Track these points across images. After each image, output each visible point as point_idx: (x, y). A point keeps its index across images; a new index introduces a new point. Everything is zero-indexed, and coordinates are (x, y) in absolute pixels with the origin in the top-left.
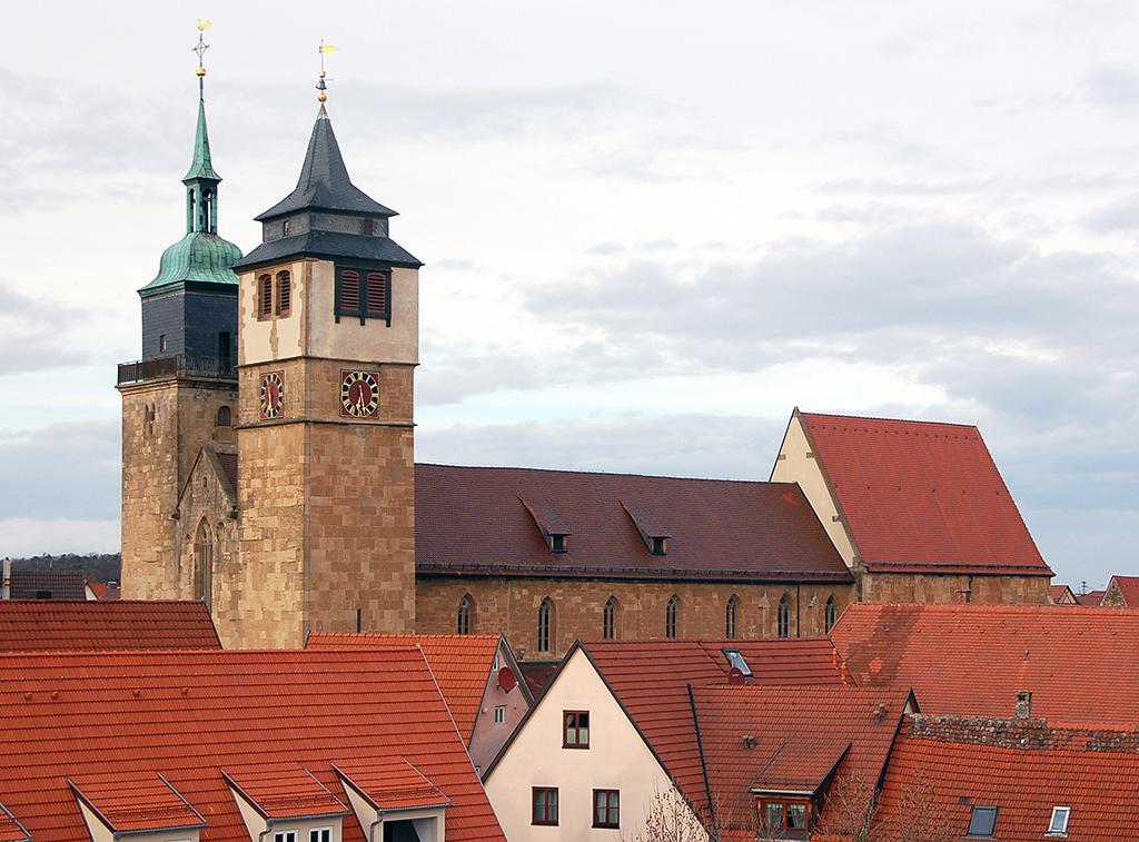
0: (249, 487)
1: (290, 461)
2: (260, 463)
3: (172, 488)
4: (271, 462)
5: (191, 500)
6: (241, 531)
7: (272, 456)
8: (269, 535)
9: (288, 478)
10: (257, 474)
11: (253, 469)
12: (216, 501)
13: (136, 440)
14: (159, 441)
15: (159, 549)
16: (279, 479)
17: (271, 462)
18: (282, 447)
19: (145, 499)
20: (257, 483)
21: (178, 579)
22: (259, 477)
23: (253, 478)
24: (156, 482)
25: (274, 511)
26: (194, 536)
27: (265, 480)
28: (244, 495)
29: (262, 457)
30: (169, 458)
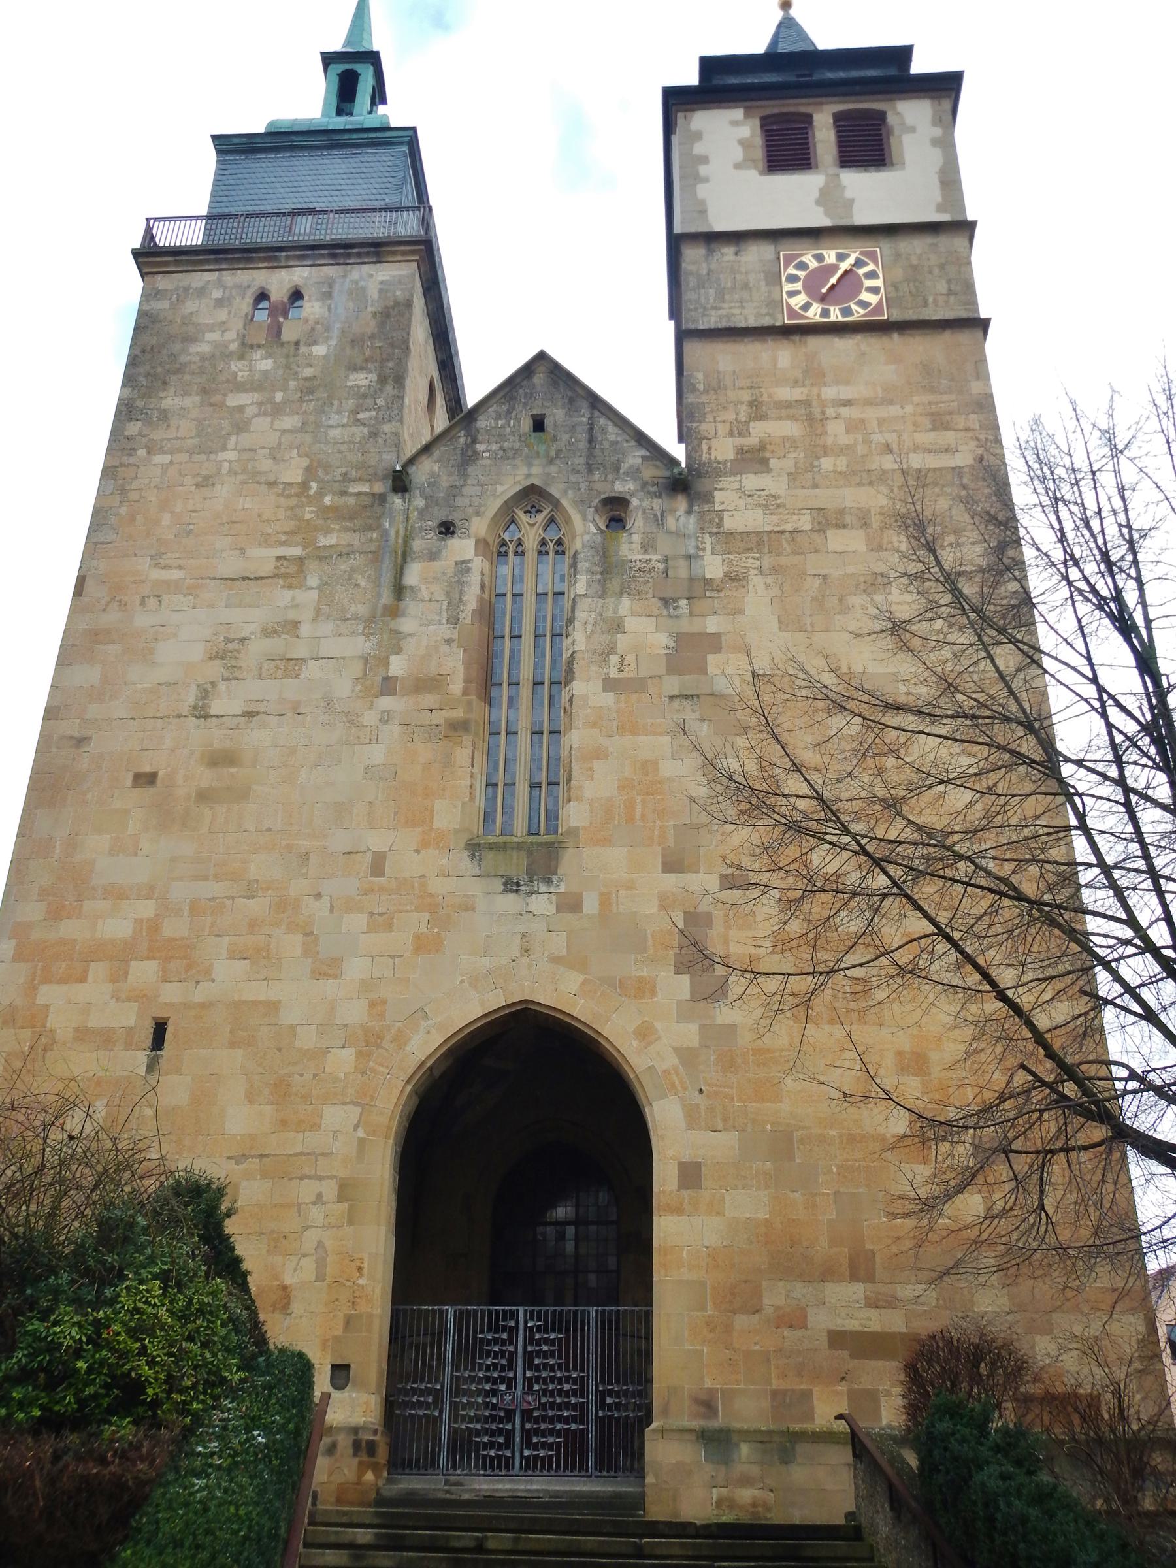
4: (829, 393)
6: (712, 523)
8: (848, 519)
14: (320, 350)
15: (296, 551)
16: (881, 422)
21: (394, 612)
23: (761, 417)
26: (480, 526)
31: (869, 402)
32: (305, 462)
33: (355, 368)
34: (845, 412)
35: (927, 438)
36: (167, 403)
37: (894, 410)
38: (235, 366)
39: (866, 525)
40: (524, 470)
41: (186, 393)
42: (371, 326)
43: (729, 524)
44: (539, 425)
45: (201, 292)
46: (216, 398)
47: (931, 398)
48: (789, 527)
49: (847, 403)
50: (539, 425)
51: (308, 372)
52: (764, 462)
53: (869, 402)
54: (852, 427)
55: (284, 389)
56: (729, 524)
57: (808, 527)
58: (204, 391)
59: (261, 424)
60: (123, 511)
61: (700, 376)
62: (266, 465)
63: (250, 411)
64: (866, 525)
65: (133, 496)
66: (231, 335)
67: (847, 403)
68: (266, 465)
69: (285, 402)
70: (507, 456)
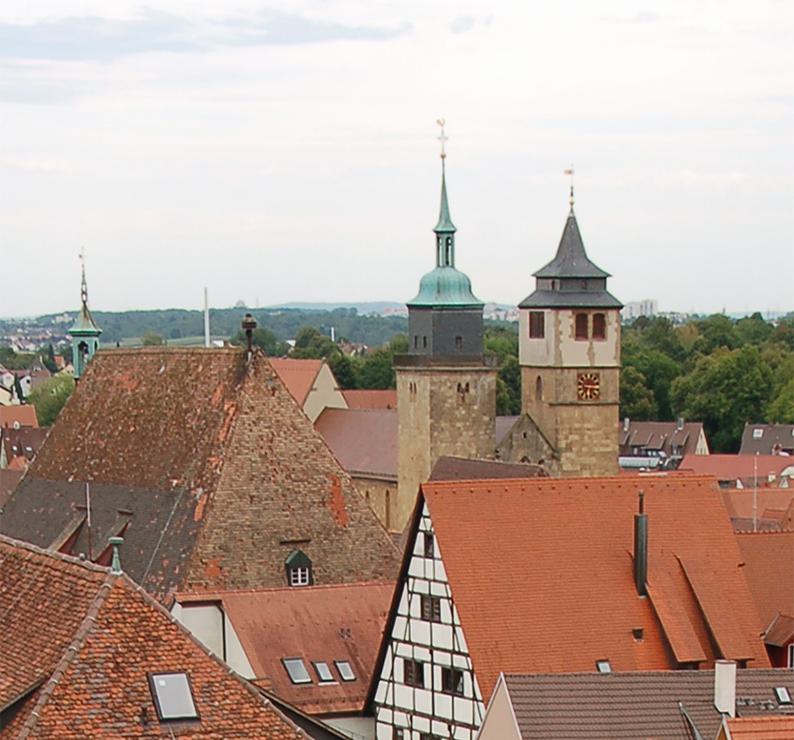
0: (566, 438)
1: (606, 426)
2: (577, 425)
4: (587, 425)
6: (560, 466)
7: (589, 422)
10: (573, 432)
13: (447, 405)
14: (475, 407)
17: (587, 425)
19: (459, 444)
23: (571, 433)
24: (471, 433)
27: (582, 436)
29: (579, 422)
31: (594, 429)
34: (589, 432)
35: (604, 442)
36: (443, 425)
37: (600, 432)
38: (457, 412)
39: (590, 468)
42: (487, 399)
43: (564, 468)
44: (525, 435)
49: (589, 429)
50: (525, 435)
51: (474, 415)
53: (594, 429)
54: (590, 437)
56: (564, 468)
58: (450, 421)
67: (589, 429)
70: (519, 447)
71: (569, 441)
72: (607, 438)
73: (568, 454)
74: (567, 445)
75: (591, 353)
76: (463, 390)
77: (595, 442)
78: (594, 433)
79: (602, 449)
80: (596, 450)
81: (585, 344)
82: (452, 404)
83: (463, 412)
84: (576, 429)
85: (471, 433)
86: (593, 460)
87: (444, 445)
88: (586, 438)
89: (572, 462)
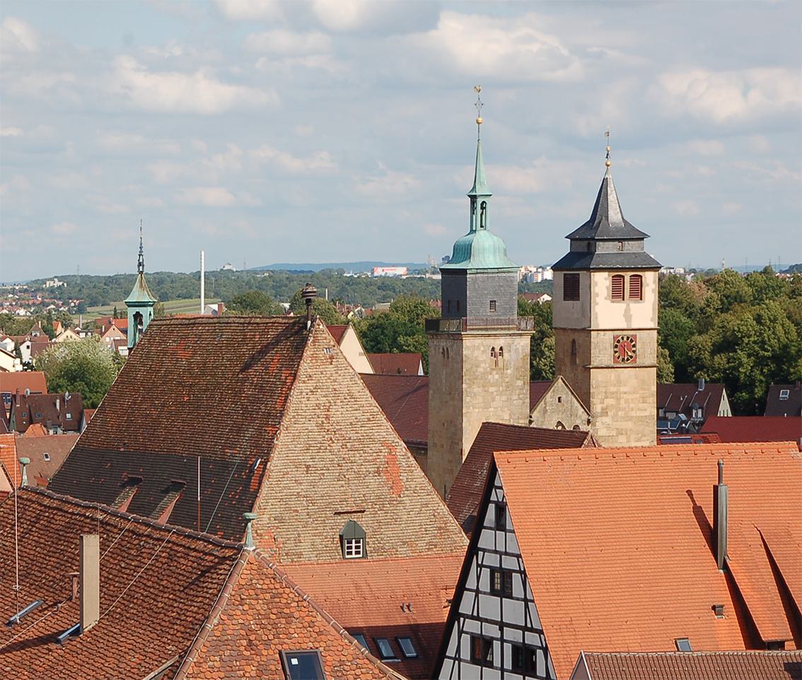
1: (643, 389)
2: (613, 389)
3: (524, 403)
4: (623, 389)
5: (545, 411)
7: (625, 385)
8: (623, 432)
9: (641, 400)
10: (609, 395)
11: (606, 393)
12: (571, 411)
13: (481, 370)
14: (509, 372)
16: (632, 399)
17: (623, 389)
18: (635, 380)
19: (491, 409)
20: (610, 401)
22: (613, 398)
23: (606, 398)
24: (504, 398)
25: (631, 419)
27: (618, 399)
28: (597, 407)
30: (520, 383)
32: (509, 412)
33: (518, 379)
35: (641, 405)
36: (476, 390)
38: (490, 377)
40: (557, 416)
41: (479, 387)
45: (478, 348)
46: (487, 389)
47: (643, 392)
48: (611, 435)
49: (625, 393)
51: (507, 380)
52: (607, 413)
54: (627, 401)
55: (502, 386)
57: (615, 434)
59: (498, 397)
60: (470, 428)
61: (594, 382)
62: (500, 413)
63: (495, 393)
64: (627, 434)
65: (472, 423)
66: (487, 365)
67: (625, 393)
68: (500, 413)
69: (503, 391)
71: (604, 405)
72: (644, 402)
73: (604, 419)
74: (602, 409)
75: (628, 316)
76: (496, 353)
77: (632, 405)
78: (630, 397)
79: (639, 414)
80: (633, 414)
81: (620, 306)
82: (485, 369)
83: (497, 377)
84: (613, 393)
85: (504, 398)
86: (630, 425)
87: (477, 410)
88: (622, 401)
89: (608, 427)
